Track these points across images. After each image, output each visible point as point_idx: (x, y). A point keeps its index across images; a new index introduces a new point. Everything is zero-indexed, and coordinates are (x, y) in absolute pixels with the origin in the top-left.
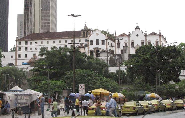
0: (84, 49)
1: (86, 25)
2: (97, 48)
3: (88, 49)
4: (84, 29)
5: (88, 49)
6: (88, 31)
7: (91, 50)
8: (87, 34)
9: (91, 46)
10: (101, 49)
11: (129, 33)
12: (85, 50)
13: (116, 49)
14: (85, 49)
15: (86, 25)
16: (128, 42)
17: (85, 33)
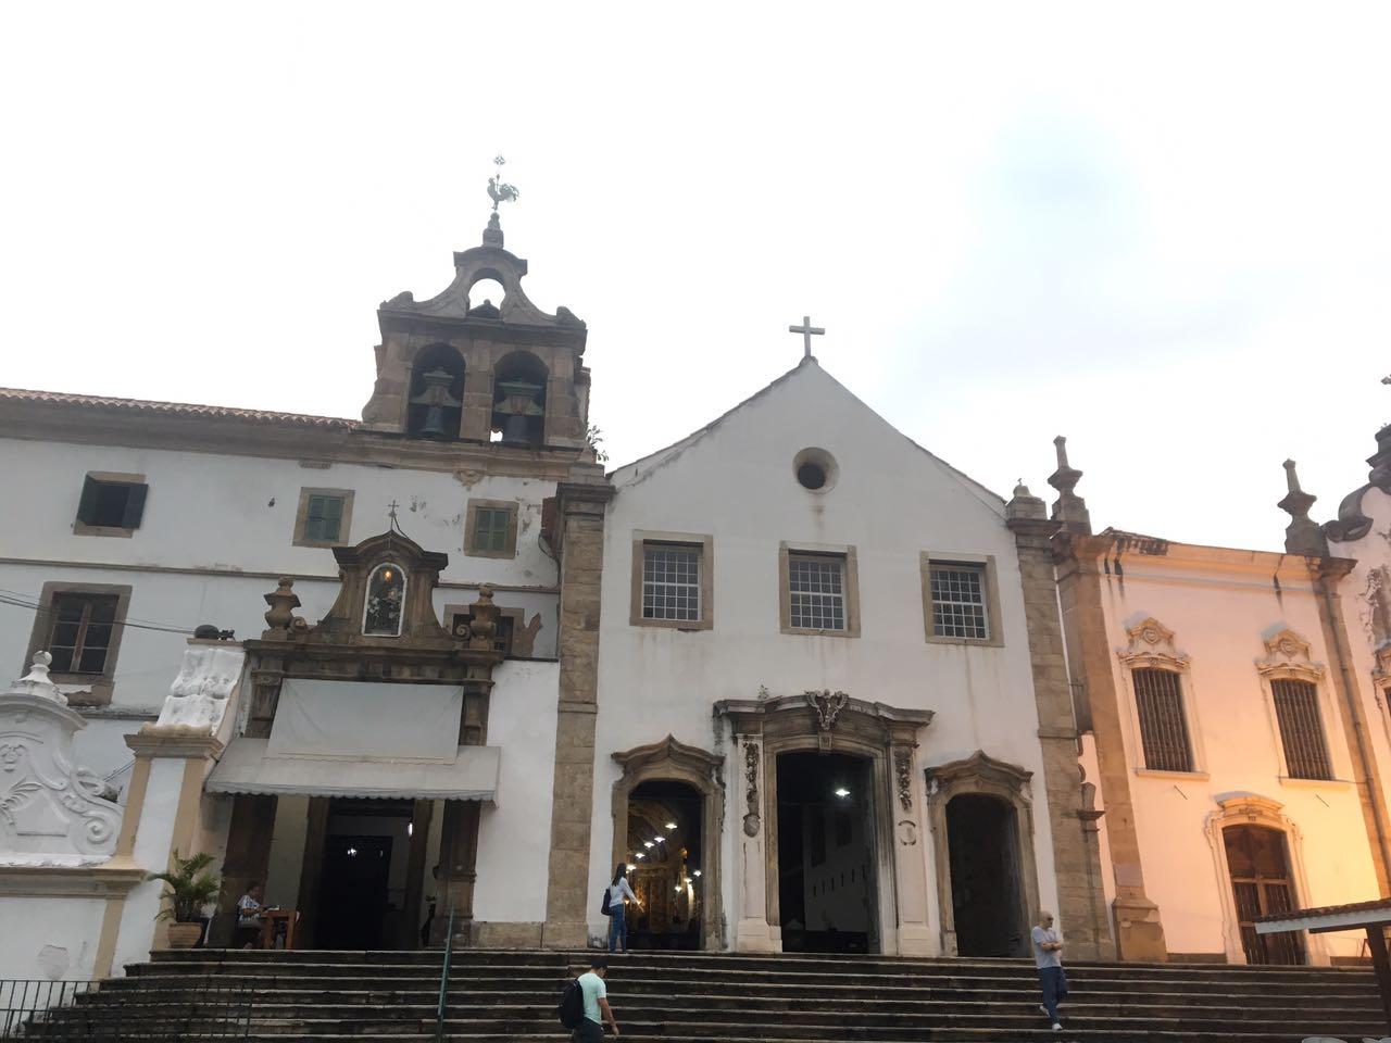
0: (442, 704)
1: (494, 234)
2: (818, 709)
3: (578, 705)
4: (458, 291)
5: (578, 705)
6: (540, 352)
7: (670, 750)
8: (500, 396)
9: (665, 641)
10: (933, 751)
11: (1297, 502)
12: (472, 732)
13: (1117, 785)
14: (476, 701)
15: (494, 234)
16: (1321, 654)
17: (457, 390)
